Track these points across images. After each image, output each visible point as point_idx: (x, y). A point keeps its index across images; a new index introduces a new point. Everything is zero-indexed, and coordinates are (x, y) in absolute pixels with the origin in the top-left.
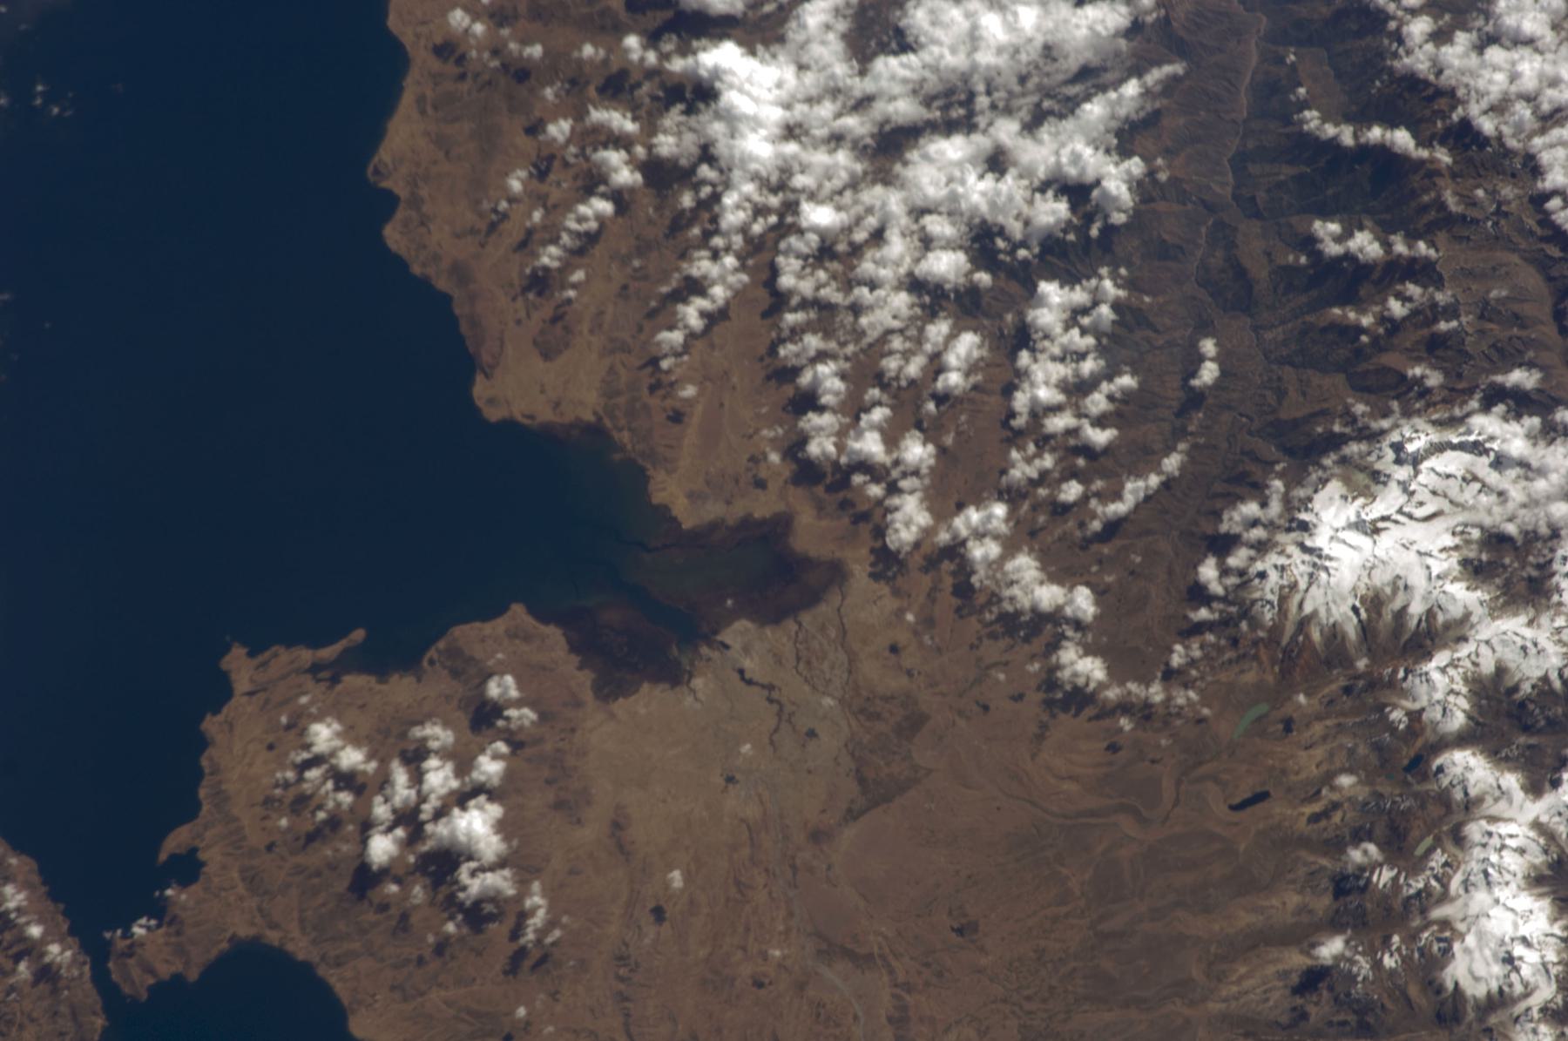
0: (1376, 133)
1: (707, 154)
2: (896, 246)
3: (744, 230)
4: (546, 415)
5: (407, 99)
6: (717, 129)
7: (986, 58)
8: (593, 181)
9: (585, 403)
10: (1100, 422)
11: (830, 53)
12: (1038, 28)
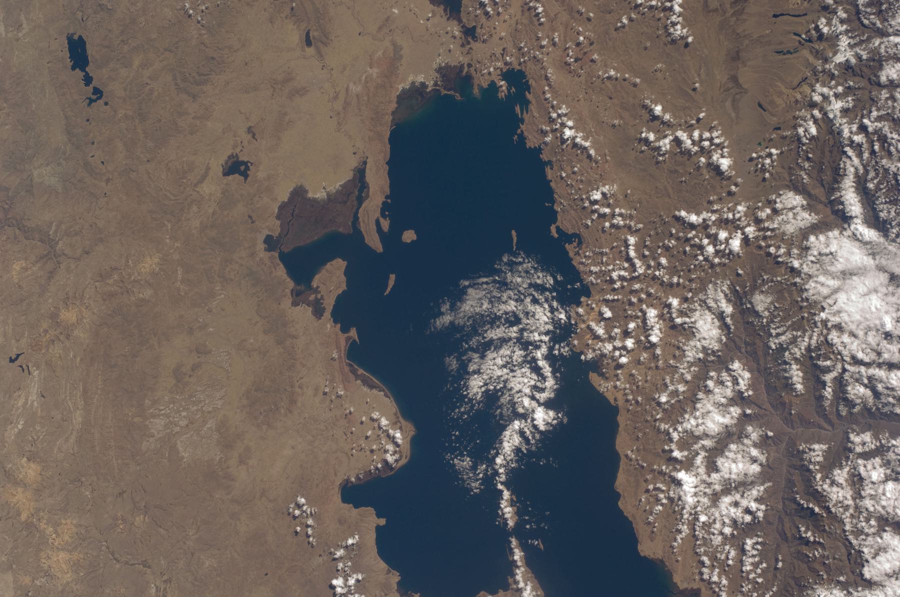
0: (811, 506)
1: (680, 498)
2: (718, 525)
3: (688, 519)
4: (652, 556)
5: (621, 468)
6: (682, 493)
7: (733, 476)
8: (658, 501)
9: (659, 554)
10: (760, 576)
11: (702, 470)
12: (743, 469)
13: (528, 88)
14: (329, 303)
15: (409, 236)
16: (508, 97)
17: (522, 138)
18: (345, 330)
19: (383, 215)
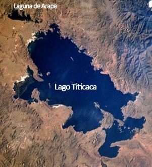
13: (58, 26)
14: (38, 98)
15: (48, 74)
16: (54, 31)
17: (62, 38)
18: (45, 100)
19: (39, 73)
